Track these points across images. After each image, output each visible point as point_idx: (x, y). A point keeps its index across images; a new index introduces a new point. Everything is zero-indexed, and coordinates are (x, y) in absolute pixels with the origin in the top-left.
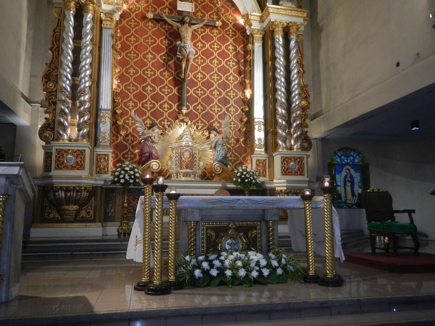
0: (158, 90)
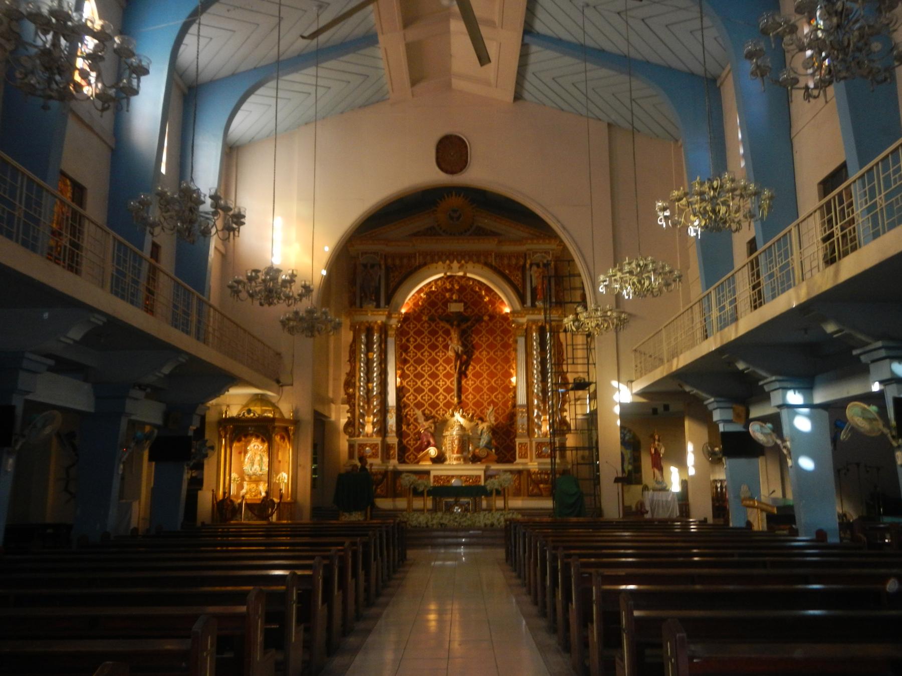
0: (434, 383)
